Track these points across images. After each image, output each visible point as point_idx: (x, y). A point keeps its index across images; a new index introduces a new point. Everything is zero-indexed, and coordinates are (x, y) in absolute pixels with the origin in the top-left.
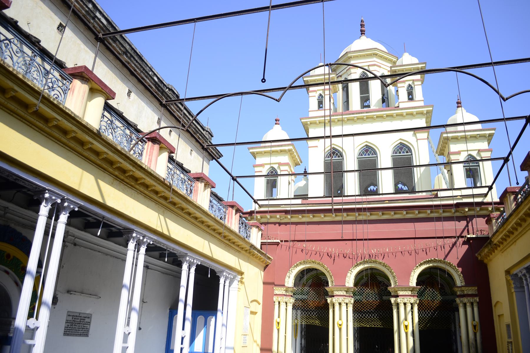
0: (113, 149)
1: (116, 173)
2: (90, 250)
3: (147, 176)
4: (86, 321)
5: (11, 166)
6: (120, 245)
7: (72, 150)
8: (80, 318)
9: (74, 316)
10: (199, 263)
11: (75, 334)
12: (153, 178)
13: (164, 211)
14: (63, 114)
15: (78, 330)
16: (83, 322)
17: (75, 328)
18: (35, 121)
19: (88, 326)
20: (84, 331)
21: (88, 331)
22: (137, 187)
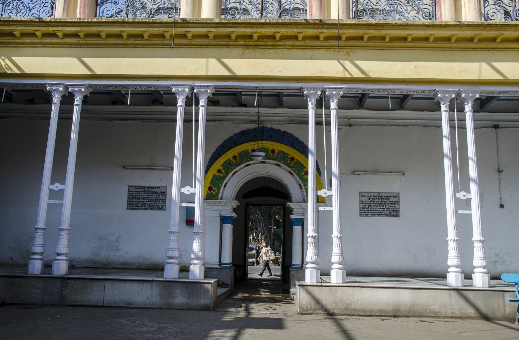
0: (212, 25)
1: (241, 42)
2: (376, 126)
3: (279, 28)
4: (391, 200)
5: (133, 81)
6: (423, 111)
7: (181, 46)
8: (380, 198)
9: (370, 196)
10: (478, 96)
11: (378, 215)
12: (289, 26)
13: (347, 53)
14: (129, 25)
15: (382, 210)
16: (386, 202)
17: (376, 208)
18: (134, 42)
19: (397, 206)
20: (391, 211)
21: (398, 211)
22: (281, 43)
